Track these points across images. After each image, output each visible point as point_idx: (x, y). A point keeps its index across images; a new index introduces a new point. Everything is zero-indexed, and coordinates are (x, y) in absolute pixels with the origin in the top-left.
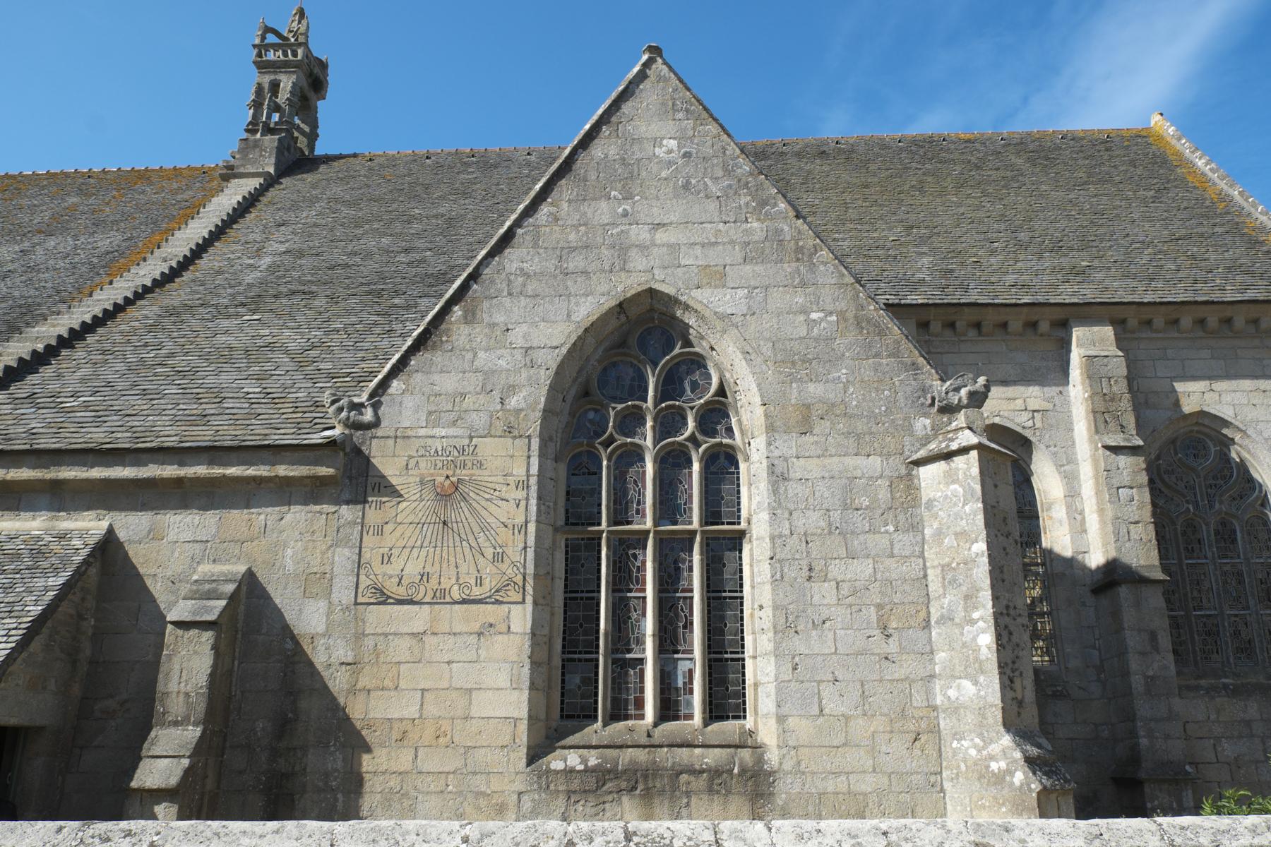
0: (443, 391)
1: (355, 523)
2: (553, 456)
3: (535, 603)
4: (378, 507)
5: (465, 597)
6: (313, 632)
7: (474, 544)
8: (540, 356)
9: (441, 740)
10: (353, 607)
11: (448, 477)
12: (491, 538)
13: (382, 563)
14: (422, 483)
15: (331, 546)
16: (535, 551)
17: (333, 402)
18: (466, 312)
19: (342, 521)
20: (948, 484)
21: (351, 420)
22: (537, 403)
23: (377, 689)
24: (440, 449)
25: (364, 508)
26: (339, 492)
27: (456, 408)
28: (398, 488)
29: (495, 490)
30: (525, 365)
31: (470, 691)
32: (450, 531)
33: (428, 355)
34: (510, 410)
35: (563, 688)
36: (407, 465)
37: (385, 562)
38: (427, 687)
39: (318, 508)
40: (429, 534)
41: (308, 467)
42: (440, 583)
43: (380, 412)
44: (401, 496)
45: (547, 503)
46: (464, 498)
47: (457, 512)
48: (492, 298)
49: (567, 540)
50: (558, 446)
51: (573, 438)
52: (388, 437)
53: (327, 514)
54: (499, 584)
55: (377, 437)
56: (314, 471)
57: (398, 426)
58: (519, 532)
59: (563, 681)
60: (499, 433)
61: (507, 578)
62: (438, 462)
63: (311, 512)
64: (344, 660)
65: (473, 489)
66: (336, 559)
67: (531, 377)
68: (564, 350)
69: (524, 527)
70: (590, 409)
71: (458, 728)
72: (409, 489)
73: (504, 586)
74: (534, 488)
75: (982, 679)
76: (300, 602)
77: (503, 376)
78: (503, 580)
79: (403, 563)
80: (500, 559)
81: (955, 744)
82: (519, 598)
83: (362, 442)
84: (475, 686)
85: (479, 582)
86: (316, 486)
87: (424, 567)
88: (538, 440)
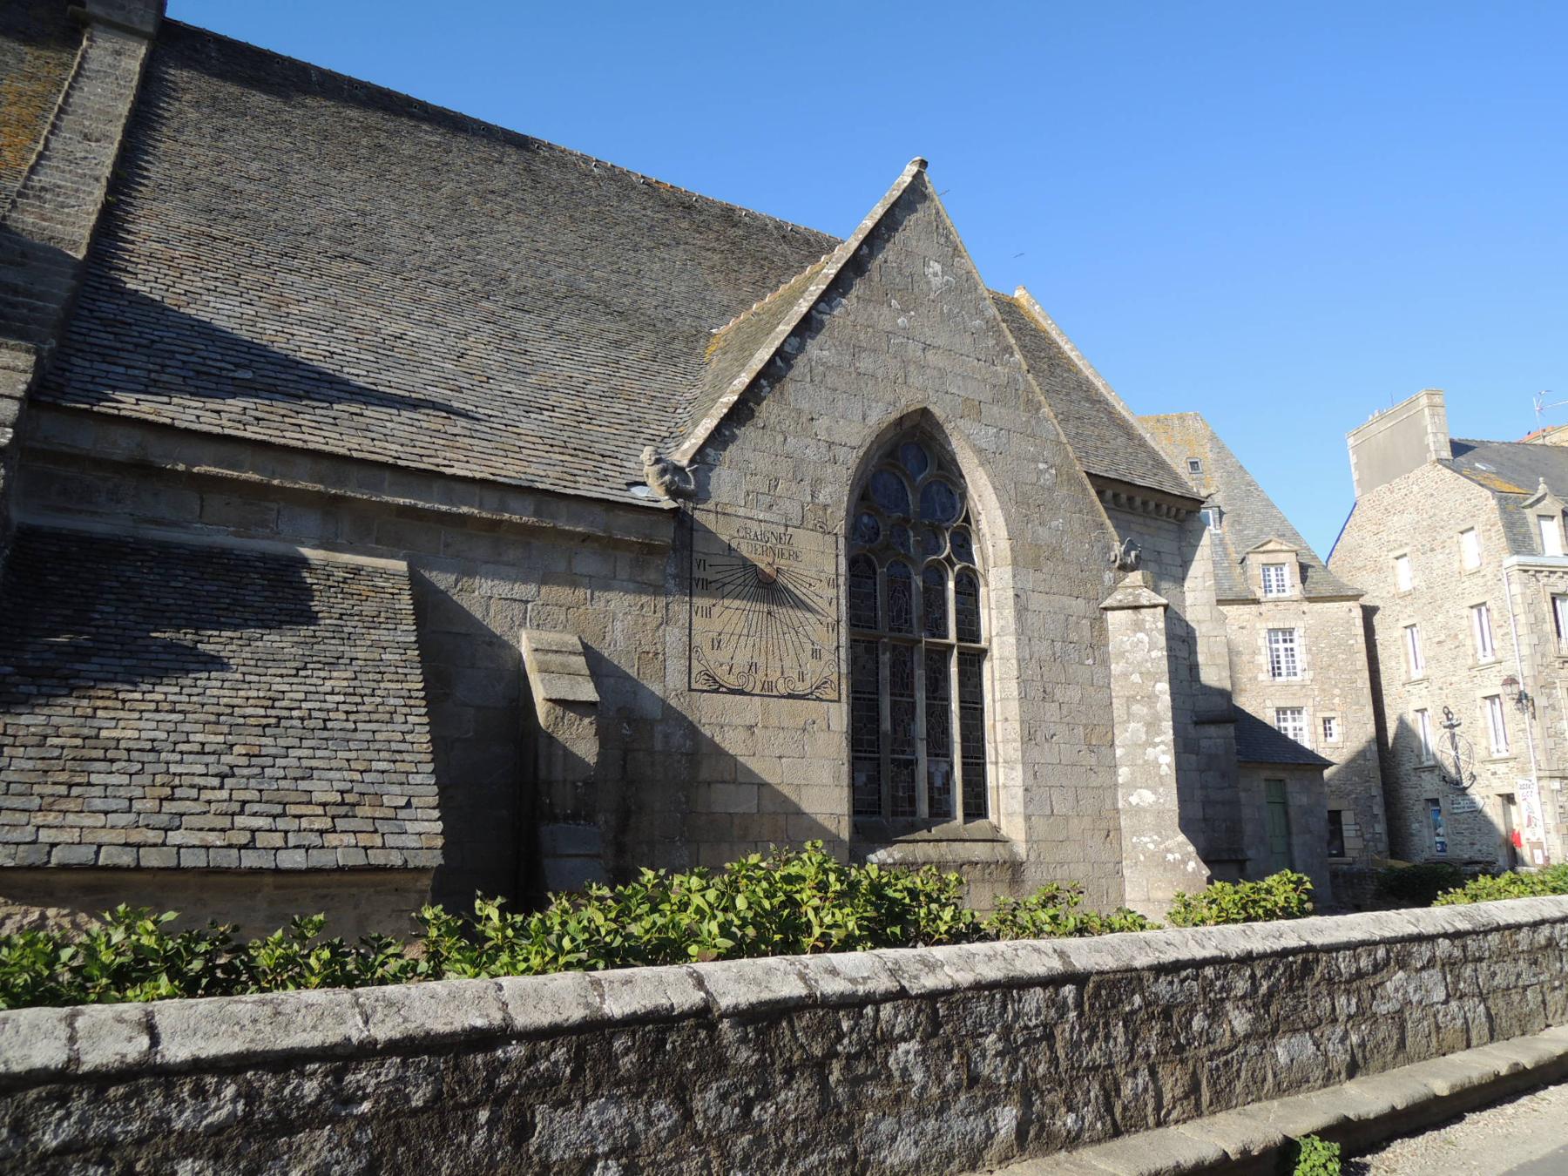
8: (841, 453)
20: (1135, 632)
40: (754, 623)
66: (668, 638)
74: (842, 588)
75: (1161, 790)
81: (1134, 840)
82: (834, 696)
84: (803, 782)
85: (802, 677)
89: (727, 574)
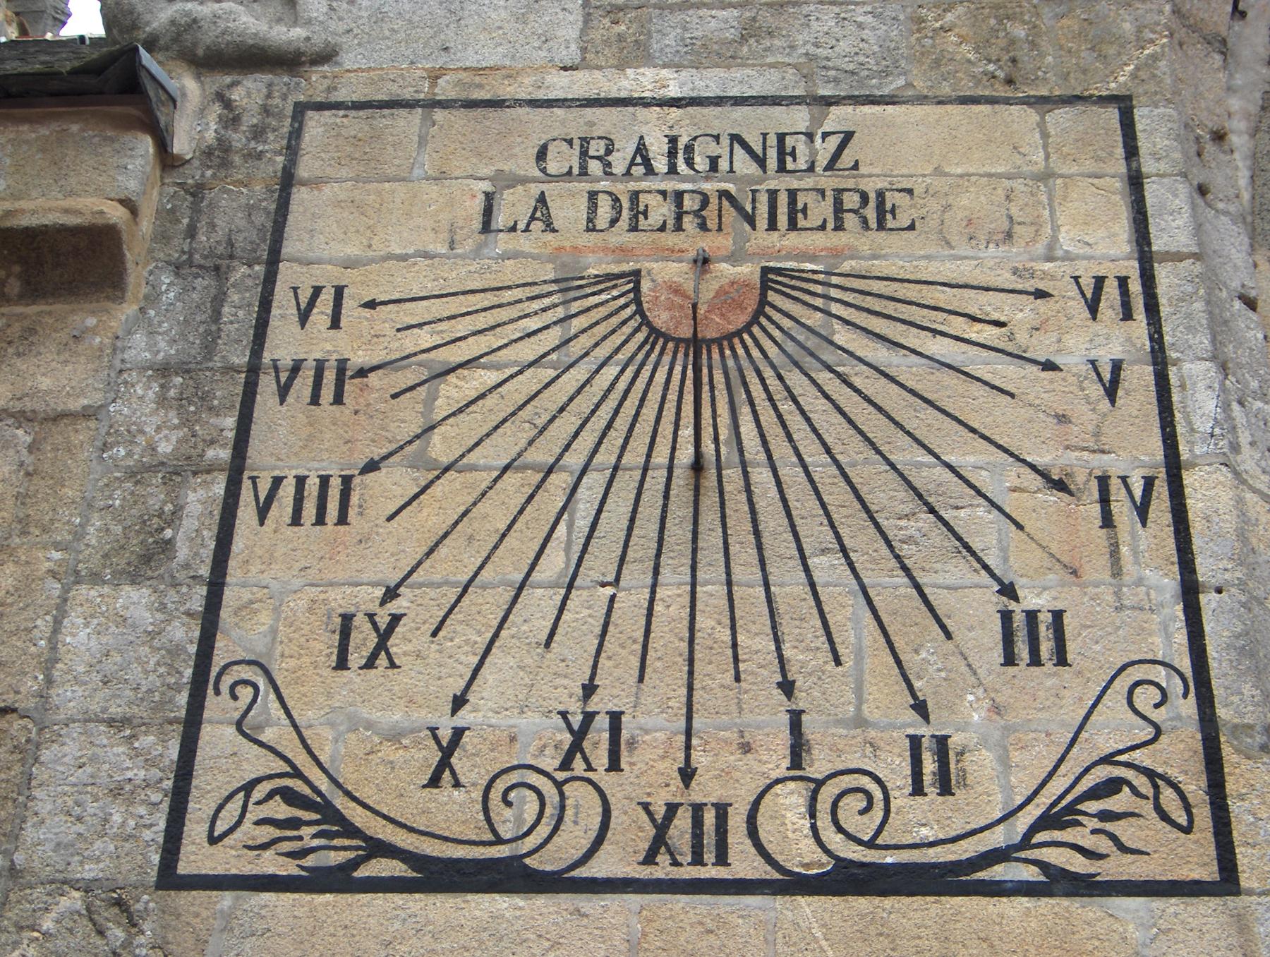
4: (327, 393)
13: (342, 664)
24: (657, 148)
37: (356, 658)
42: (687, 774)
47: (767, 417)
58: (1142, 511)
62: (651, 200)
69: (1161, 489)
73: (1093, 794)
80: (1046, 647)
87: (589, 689)
89: (462, 326)
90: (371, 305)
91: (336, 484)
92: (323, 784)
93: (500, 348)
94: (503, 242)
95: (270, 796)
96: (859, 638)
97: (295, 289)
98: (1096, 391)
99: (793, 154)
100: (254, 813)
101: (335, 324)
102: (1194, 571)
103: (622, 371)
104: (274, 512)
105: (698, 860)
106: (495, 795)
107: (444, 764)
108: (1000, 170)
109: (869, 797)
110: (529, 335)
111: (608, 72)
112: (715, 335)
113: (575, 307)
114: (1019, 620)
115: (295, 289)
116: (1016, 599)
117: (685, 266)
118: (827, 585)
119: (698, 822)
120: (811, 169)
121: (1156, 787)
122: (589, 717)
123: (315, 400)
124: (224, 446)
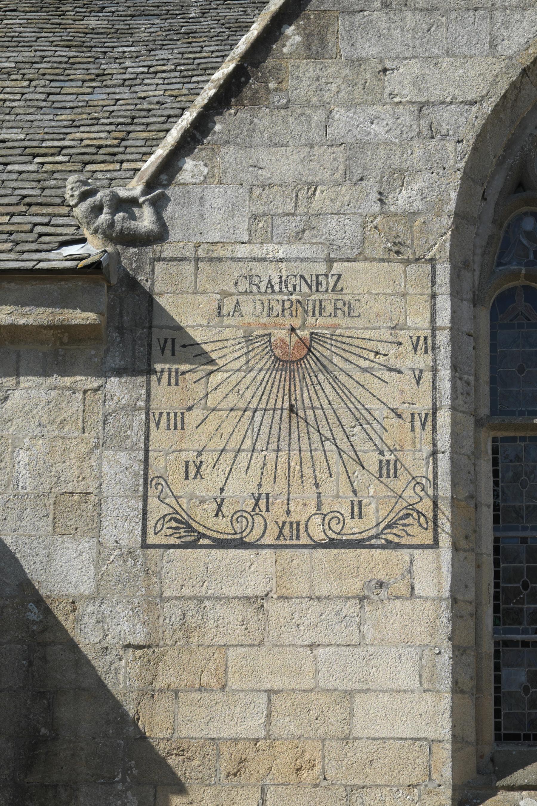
0: (276, 179)
1: (135, 409)
2: (470, 296)
3: (455, 548)
4: (173, 381)
5: (333, 536)
6: (71, 591)
7: (344, 446)
9: (304, 774)
10: (139, 552)
11: (293, 330)
12: (374, 436)
13: (187, 478)
14: (248, 339)
15: (96, 447)
16: (451, 458)
17: (84, 196)
18: (308, 37)
19: (111, 405)
21: (118, 228)
22: (442, 202)
23: (191, 689)
24: (275, 280)
25: (149, 382)
26: (102, 353)
27: (301, 210)
28: (207, 348)
29: (377, 353)
30: (420, 133)
31: (350, 694)
32: (302, 423)
33: (244, 114)
34: (396, 214)
35: (497, 689)
36: (220, 308)
37: (192, 475)
38: (275, 687)
39: (67, 381)
40: (265, 428)
41: (50, 310)
42: (288, 512)
43: (166, 216)
44: (212, 362)
45: (466, 377)
46: (324, 367)
47: (312, 391)
48: (354, 12)
49: (494, 440)
50: (476, 277)
51: (499, 264)
52: (183, 259)
53: (85, 392)
54: (392, 515)
55: (164, 259)
56: (61, 317)
57: (200, 239)
58: (423, 425)
59: (497, 679)
60: (379, 253)
61: (405, 504)
62: (274, 303)
63: (56, 388)
64: (129, 640)
65: (337, 351)
66: (106, 468)
67: (431, 155)
68: (488, 107)
69: (430, 418)
70: (526, 214)
71: (333, 755)
72: (226, 351)
73: (401, 518)
76: (47, 542)
77: (382, 153)
78: (398, 507)
79: (223, 478)
80: (392, 472)
82: (427, 538)
83: (138, 267)
84: (357, 686)
86: (62, 343)
87: (260, 485)
88: (447, 266)
90: (184, 346)
91: (179, 414)
92: (185, 516)
93: (226, 364)
94: (227, 321)
95: (170, 520)
96: (338, 469)
97: (159, 339)
98: (414, 381)
99: (321, 284)
100: (166, 526)
101: (173, 354)
102: (436, 446)
103: (266, 373)
104: (161, 425)
105: (291, 539)
106: (235, 518)
107: (219, 509)
108: (390, 292)
109: (339, 520)
110: (236, 359)
111: (257, 245)
112: (295, 359)
113: (250, 348)
114: (384, 463)
115: (159, 339)
116: (383, 455)
117: (285, 331)
118: (329, 451)
119: (291, 527)
120: (327, 291)
121: (419, 516)
122: (260, 495)
123: (169, 384)
124: (142, 401)
